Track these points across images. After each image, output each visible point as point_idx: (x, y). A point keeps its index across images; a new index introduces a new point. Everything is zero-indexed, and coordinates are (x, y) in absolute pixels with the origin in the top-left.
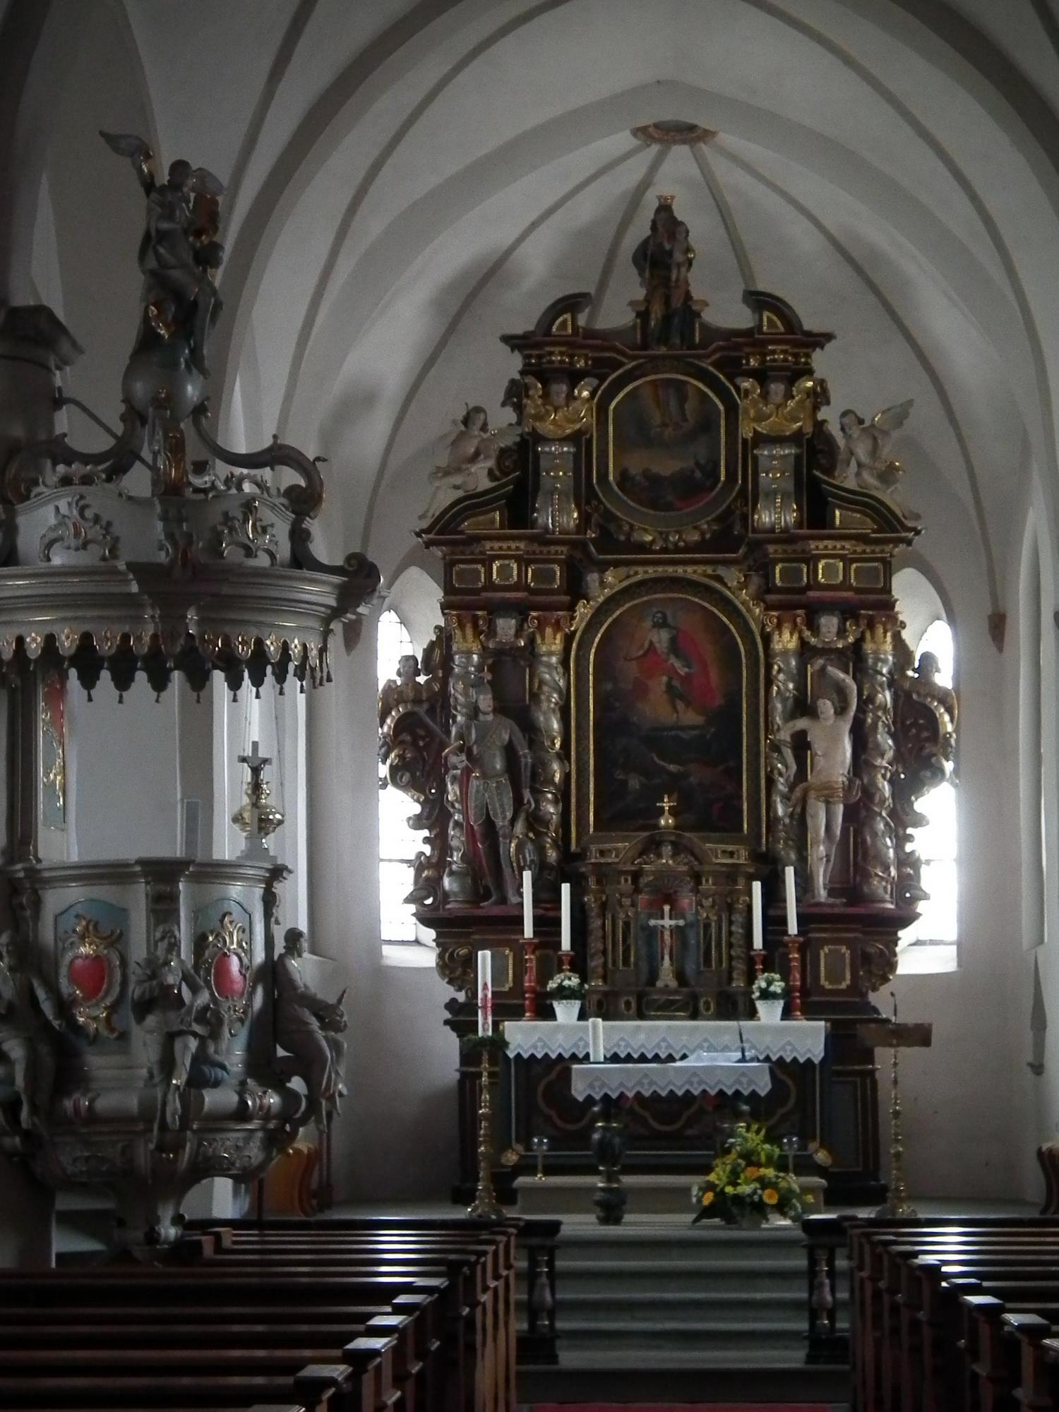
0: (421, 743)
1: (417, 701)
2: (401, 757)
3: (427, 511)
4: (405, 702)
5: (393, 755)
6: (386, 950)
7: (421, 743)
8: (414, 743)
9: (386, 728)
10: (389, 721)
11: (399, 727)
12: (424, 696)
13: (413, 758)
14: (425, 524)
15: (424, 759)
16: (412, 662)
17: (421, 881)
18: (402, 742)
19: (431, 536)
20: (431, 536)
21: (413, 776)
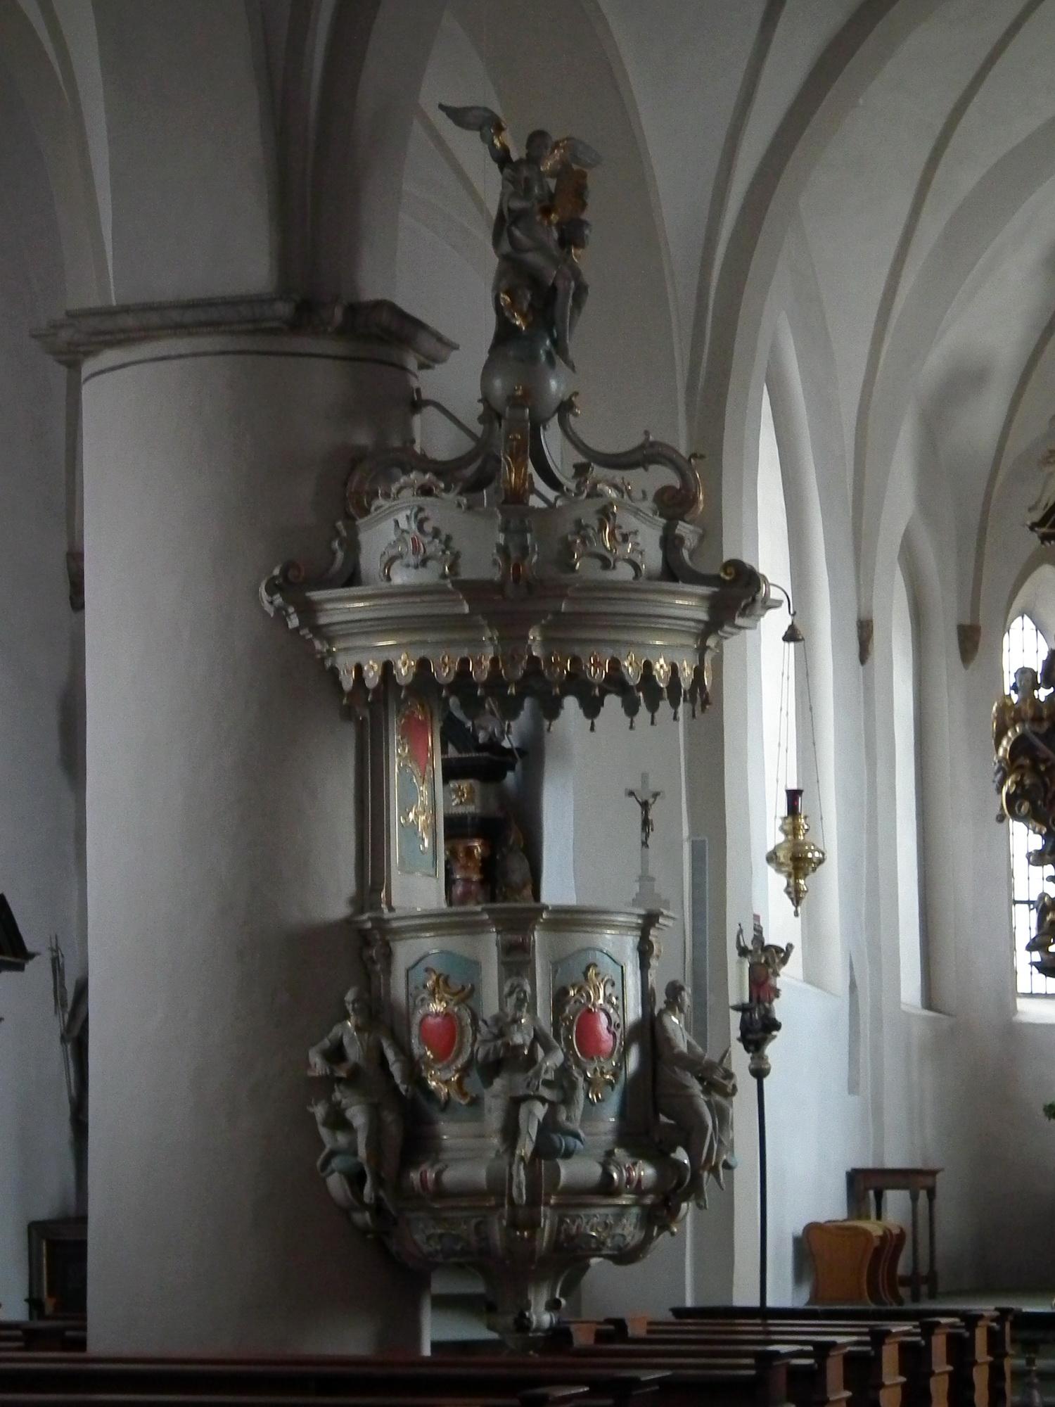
0: (1042, 768)
1: (1037, 719)
2: (1019, 784)
3: (1039, 500)
4: (1023, 721)
5: (1009, 782)
6: (1022, 1004)
7: (1042, 768)
8: (1034, 768)
9: (1001, 751)
10: (1004, 742)
11: (1019, 747)
12: (1045, 713)
13: (1033, 785)
14: (1036, 516)
15: (1045, 784)
16: (1029, 675)
17: (1046, 925)
18: (1021, 767)
19: (1044, 530)
20: (1044, 530)
21: (1033, 803)
